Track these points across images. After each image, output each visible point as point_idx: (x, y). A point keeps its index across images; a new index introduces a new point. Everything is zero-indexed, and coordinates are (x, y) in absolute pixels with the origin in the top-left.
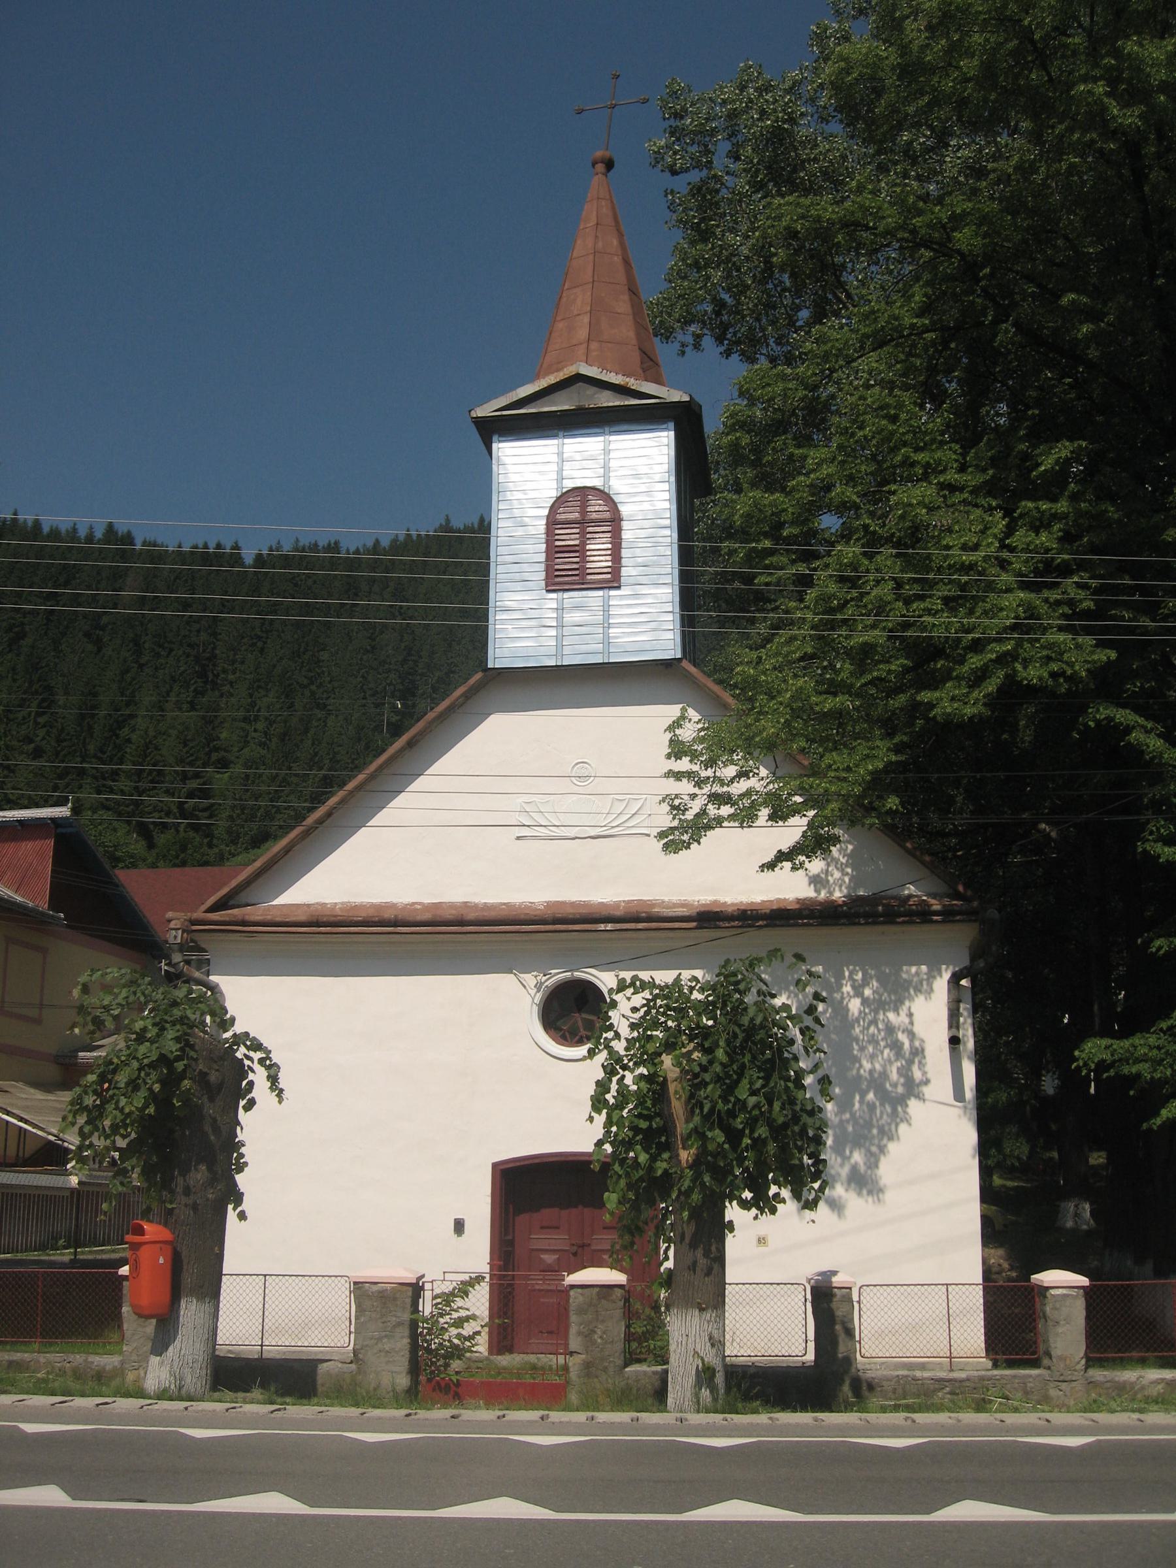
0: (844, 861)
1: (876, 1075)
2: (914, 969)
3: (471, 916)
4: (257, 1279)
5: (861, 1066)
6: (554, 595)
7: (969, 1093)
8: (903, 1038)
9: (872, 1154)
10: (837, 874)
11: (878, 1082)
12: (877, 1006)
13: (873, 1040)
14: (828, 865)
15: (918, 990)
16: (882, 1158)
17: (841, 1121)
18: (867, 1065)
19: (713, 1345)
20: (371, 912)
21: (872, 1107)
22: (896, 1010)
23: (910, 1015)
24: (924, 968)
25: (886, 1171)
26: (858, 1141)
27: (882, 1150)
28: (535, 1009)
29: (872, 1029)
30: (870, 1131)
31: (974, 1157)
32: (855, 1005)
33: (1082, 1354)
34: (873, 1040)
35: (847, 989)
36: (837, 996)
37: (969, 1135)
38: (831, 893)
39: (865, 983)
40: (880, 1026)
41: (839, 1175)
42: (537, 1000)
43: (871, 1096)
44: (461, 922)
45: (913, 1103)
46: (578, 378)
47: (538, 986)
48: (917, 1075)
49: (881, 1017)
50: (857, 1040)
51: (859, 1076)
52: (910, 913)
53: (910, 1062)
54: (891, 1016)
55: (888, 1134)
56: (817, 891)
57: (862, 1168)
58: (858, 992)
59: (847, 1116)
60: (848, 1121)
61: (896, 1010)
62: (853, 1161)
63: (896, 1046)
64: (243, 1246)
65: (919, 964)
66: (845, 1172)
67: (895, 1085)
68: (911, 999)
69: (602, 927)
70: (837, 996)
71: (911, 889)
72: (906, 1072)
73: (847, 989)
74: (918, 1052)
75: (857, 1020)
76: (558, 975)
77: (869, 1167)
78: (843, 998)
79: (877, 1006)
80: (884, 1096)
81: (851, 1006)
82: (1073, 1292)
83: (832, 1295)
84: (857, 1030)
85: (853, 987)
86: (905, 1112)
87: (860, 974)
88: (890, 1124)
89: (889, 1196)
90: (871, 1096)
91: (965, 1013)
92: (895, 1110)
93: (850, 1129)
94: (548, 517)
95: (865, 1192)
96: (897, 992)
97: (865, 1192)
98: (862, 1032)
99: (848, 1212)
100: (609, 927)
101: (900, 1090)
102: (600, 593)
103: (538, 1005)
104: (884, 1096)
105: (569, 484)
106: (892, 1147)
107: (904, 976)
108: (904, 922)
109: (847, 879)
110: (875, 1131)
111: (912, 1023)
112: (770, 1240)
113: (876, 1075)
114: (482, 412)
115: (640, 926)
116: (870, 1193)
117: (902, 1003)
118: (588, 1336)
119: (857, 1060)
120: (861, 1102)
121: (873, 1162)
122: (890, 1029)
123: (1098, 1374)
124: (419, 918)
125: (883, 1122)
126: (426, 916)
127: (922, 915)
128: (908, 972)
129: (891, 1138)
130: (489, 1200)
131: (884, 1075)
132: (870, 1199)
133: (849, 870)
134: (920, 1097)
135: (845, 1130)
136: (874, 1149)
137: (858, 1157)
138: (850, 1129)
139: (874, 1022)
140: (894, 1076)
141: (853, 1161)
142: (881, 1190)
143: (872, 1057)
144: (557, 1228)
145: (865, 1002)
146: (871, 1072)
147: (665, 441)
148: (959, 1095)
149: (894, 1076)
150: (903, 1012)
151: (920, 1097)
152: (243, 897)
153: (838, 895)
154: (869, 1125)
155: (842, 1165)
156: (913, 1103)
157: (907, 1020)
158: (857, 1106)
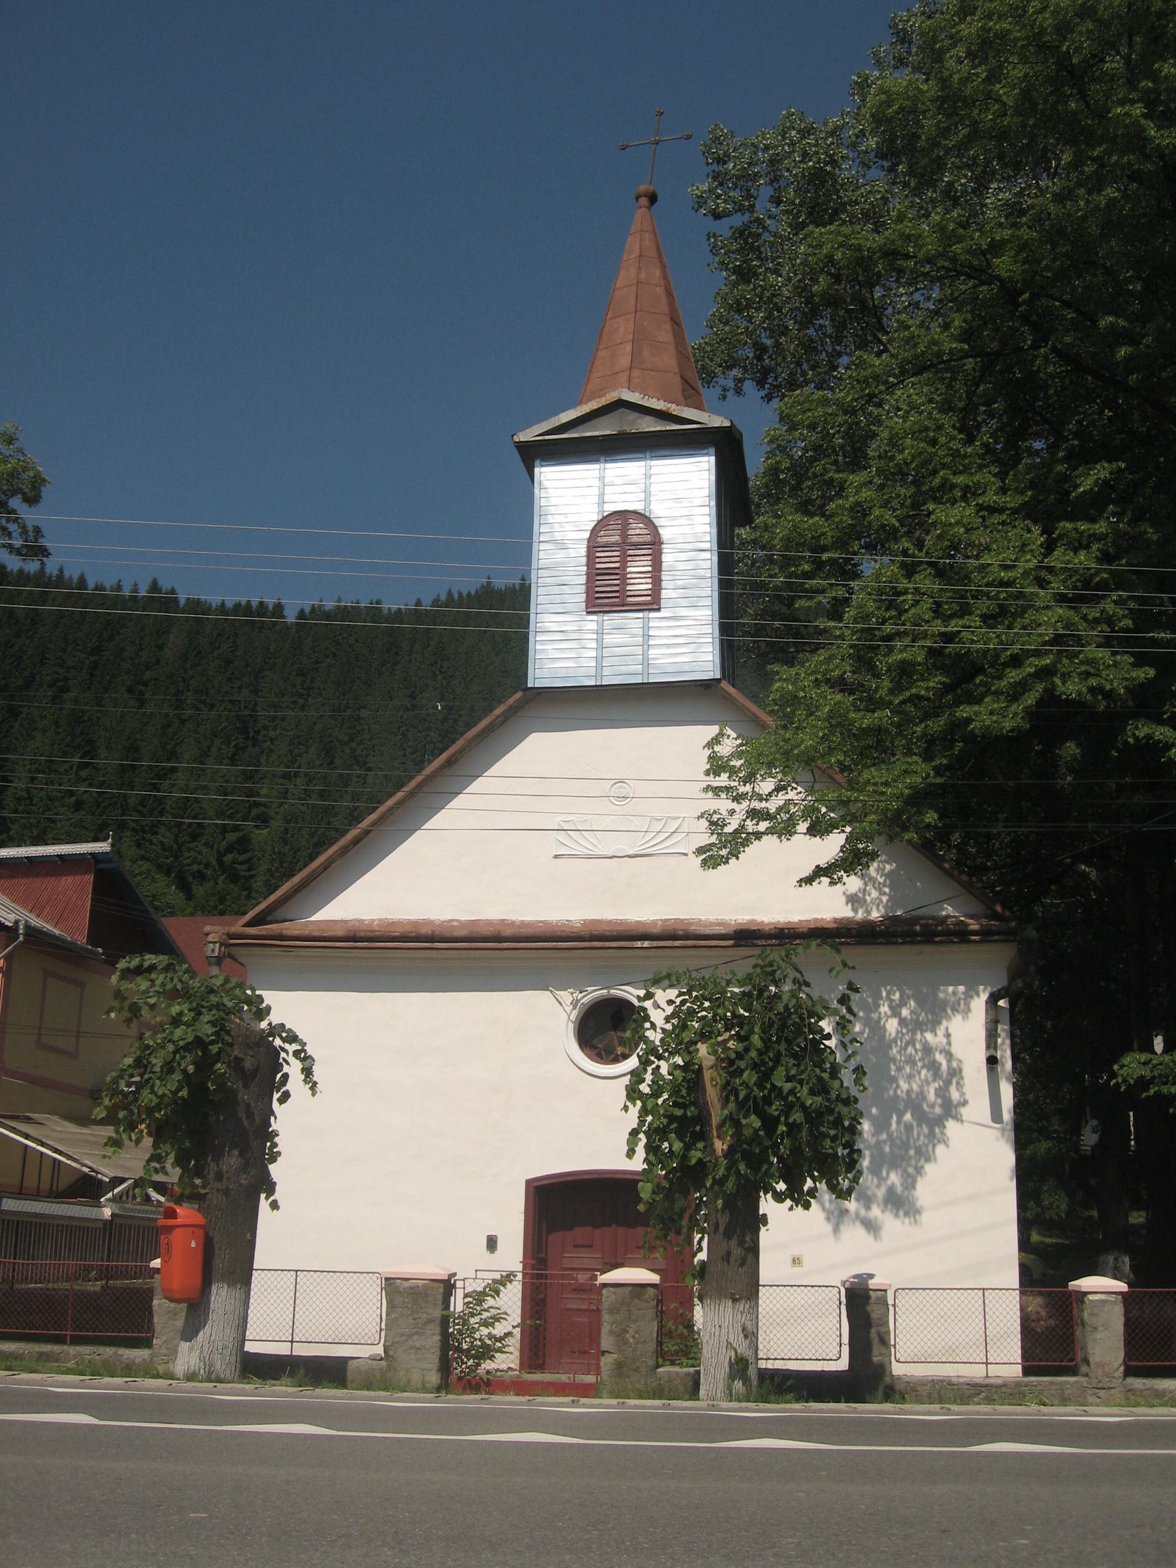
0: (881, 880)
1: (913, 1096)
2: (951, 989)
3: (508, 932)
4: (289, 1274)
5: (898, 1086)
6: (594, 617)
7: (1007, 1115)
8: (940, 1058)
9: (909, 1175)
10: (875, 894)
11: (915, 1103)
12: (914, 1026)
13: (911, 1061)
14: (866, 884)
15: (955, 1010)
16: (919, 1179)
17: (878, 1142)
18: (904, 1086)
19: (746, 1337)
20: (408, 928)
21: (909, 1127)
22: (934, 1031)
23: (948, 1035)
24: (961, 988)
25: (924, 1192)
26: (895, 1162)
27: (919, 1170)
28: (571, 1026)
29: (910, 1050)
30: (907, 1151)
31: (1011, 1179)
32: (892, 1026)
33: (1120, 1361)
34: (911, 1061)
35: (885, 1009)
36: (875, 1016)
37: (1008, 1158)
38: (869, 912)
39: (903, 1003)
40: (918, 1046)
41: (875, 1196)
42: (573, 1017)
43: (908, 1117)
44: (498, 938)
45: (950, 1124)
46: (620, 404)
47: (574, 1004)
49: (919, 1037)
50: (894, 1060)
51: (896, 1096)
52: (948, 933)
53: (948, 1083)
54: (929, 1036)
56: (855, 910)
57: (899, 1189)
58: (895, 1012)
59: (884, 1136)
60: (885, 1142)
61: (934, 1031)
62: (889, 1182)
63: (934, 1067)
64: (277, 1236)
65: (956, 984)
66: (881, 1193)
67: (932, 1106)
68: (948, 1018)
69: (639, 944)
70: (875, 1016)
71: (948, 910)
72: (943, 1093)
73: (885, 1009)
74: (956, 1073)
75: (895, 1040)
76: (594, 993)
77: (906, 1189)
78: (880, 1018)
79: (914, 1026)
80: (921, 1117)
81: (888, 1026)
82: (1112, 1298)
83: (868, 1297)
84: (894, 1050)
85: (890, 1007)
86: (942, 1133)
87: (897, 995)
88: (927, 1146)
89: (925, 1217)
90: (908, 1117)
91: (1003, 1034)
93: (887, 1149)
94: (589, 540)
95: (901, 1213)
97: (901, 1213)
98: (899, 1052)
99: (884, 1233)
100: (646, 944)
101: (938, 1110)
102: (640, 615)
103: (574, 1023)
104: (921, 1117)
105: (610, 508)
106: (928, 1168)
107: (941, 995)
108: (941, 942)
109: (885, 899)
110: (912, 1152)
111: (949, 1044)
112: (805, 1261)
113: (913, 1096)
114: (523, 437)
115: (677, 943)
116: (907, 1214)
117: (940, 1023)
118: (620, 1336)
119: (894, 1080)
120: (899, 1122)
121: (910, 1183)
122: (927, 1050)
123: (1138, 1383)
124: (456, 934)
125: (920, 1143)
126: (463, 933)
127: (960, 935)
128: (945, 991)
129: (928, 1160)
130: (522, 1217)
131: (922, 1095)
132: (907, 1221)
133: (887, 890)
134: (958, 1118)
135: (881, 1151)
136: (911, 1170)
137: (894, 1178)
138: (887, 1149)
139: (912, 1042)
140: (931, 1096)
141: (889, 1182)
142: (918, 1212)
143: (910, 1077)
144: (590, 1246)
145: (902, 1022)
146: (909, 1092)
147: (706, 466)
148: (996, 1116)
149: (931, 1096)
150: (940, 1032)
151: (958, 1118)
152: (280, 913)
153: (875, 915)
154: (906, 1146)
155: (878, 1186)
156: (950, 1124)
157: (945, 1041)
158: (894, 1126)
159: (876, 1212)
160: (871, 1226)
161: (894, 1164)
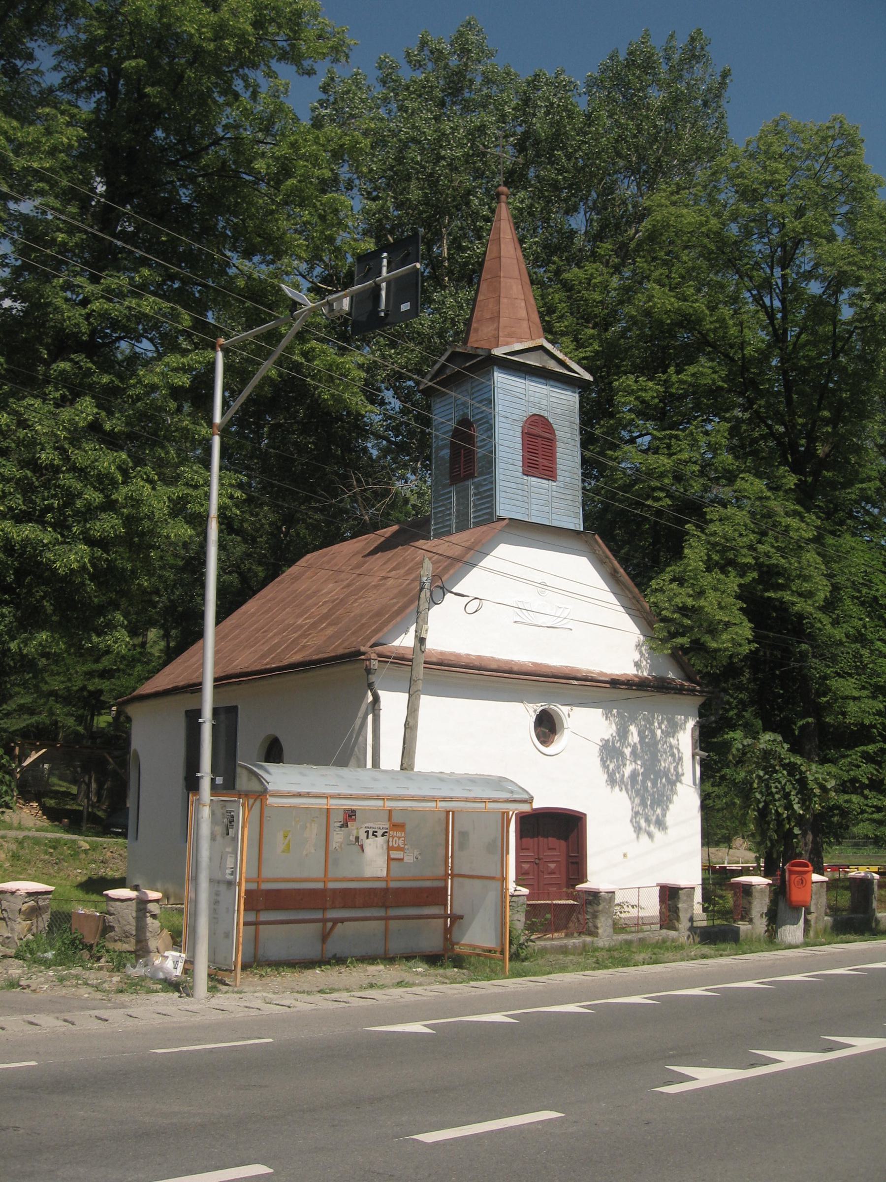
8: (675, 751)
11: (666, 773)
13: (665, 752)
25: (669, 819)
32: (659, 732)
39: (662, 722)
48: (680, 770)
55: (670, 800)
63: (673, 755)
66: (654, 818)
71: (671, 675)
72: (676, 769)
74: (681, 759)
92: (672, 790)
96: (673, 729)
106: (671, 806)
115: (588, 683)
119: (659, 761)
122: (671, 747)
131: (669, 769)
139: (666, 742)
145: (662, 732)
153: (645, 674)
159: (652, 828)
160: (650, 835)
161: (659, 805)
